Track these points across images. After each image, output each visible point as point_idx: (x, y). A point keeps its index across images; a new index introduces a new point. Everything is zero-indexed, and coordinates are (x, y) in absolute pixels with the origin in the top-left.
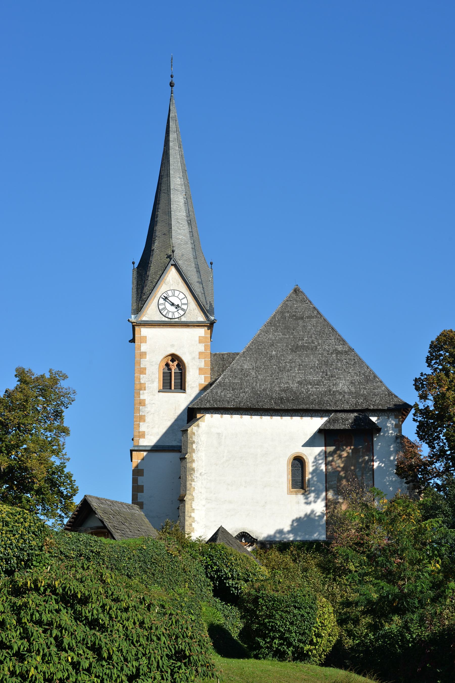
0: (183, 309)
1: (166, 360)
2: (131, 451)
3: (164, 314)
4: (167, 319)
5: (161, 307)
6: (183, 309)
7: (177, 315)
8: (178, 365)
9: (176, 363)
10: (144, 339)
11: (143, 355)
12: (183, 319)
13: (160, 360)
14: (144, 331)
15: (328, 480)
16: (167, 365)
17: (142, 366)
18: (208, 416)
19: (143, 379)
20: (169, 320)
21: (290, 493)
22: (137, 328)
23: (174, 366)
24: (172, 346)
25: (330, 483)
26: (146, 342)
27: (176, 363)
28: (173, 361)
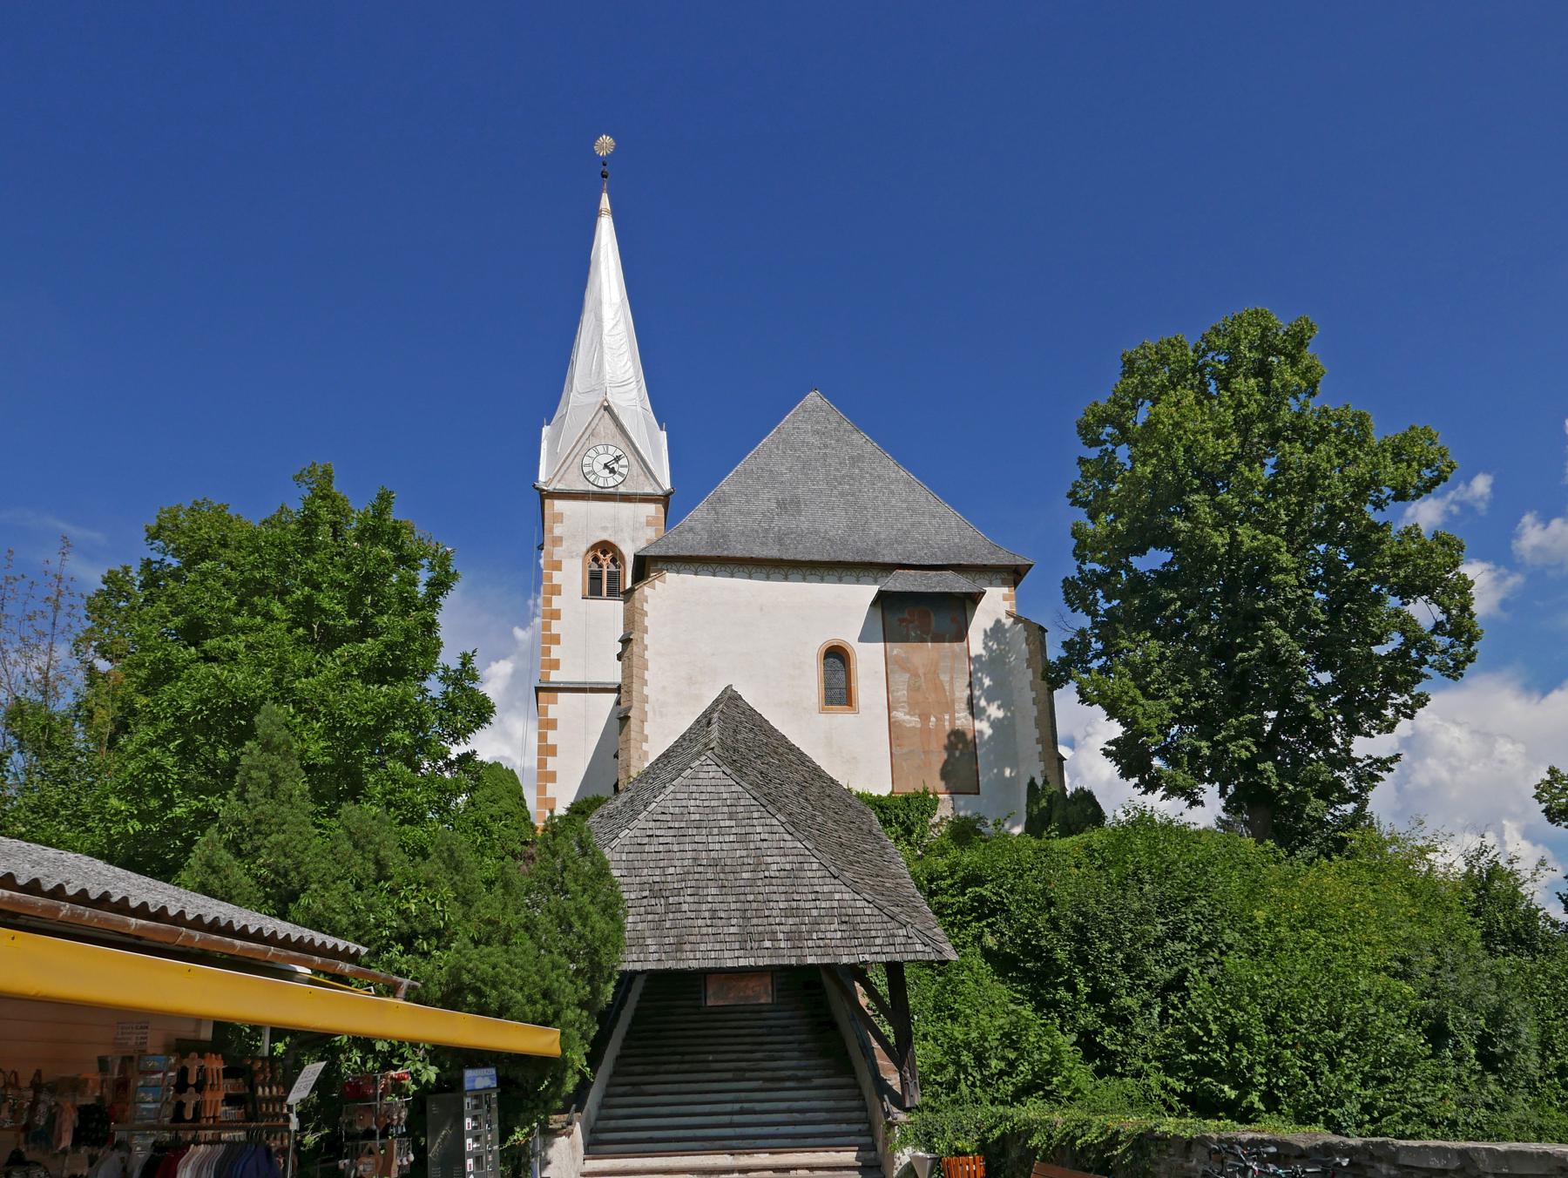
0: (620, 474)
1: (591, 554)
2: (538, 690)
3: (591, 480)
4: (595, 489)
5: (586, 470)
6: (620, 474)
7: (611, 483)
8: (613, 560)
9: (609, 556)
10: (559, 518)
11: (558, 541)
12: (622, 489)
13: (585, 550)
14: (559, 505)
15: (891, 689)
16: (596, 559)
17: (555, 558)
18: (671, 577)
19: (557, 577)
20: (600, 490)
21: (822, 711)
22: (547, 501)
23: (606, 561)
24: (605, 529)
25: (895, 694)
26: (562, 522)
27: (609, 556)
28: (605, 553)
